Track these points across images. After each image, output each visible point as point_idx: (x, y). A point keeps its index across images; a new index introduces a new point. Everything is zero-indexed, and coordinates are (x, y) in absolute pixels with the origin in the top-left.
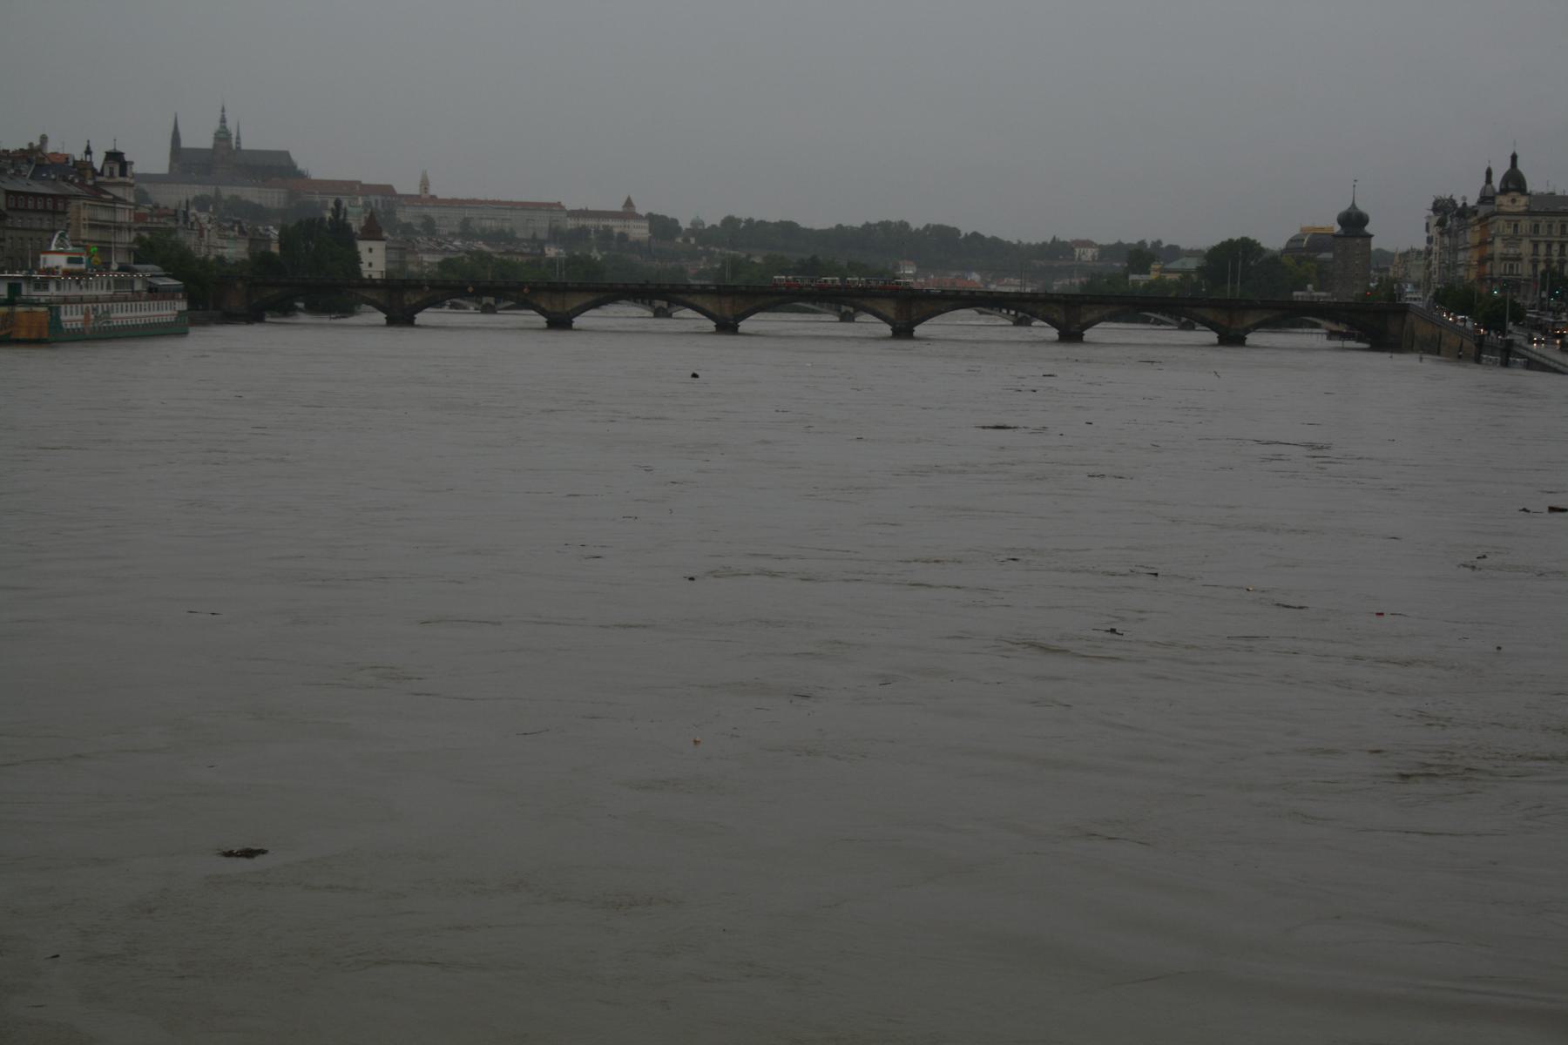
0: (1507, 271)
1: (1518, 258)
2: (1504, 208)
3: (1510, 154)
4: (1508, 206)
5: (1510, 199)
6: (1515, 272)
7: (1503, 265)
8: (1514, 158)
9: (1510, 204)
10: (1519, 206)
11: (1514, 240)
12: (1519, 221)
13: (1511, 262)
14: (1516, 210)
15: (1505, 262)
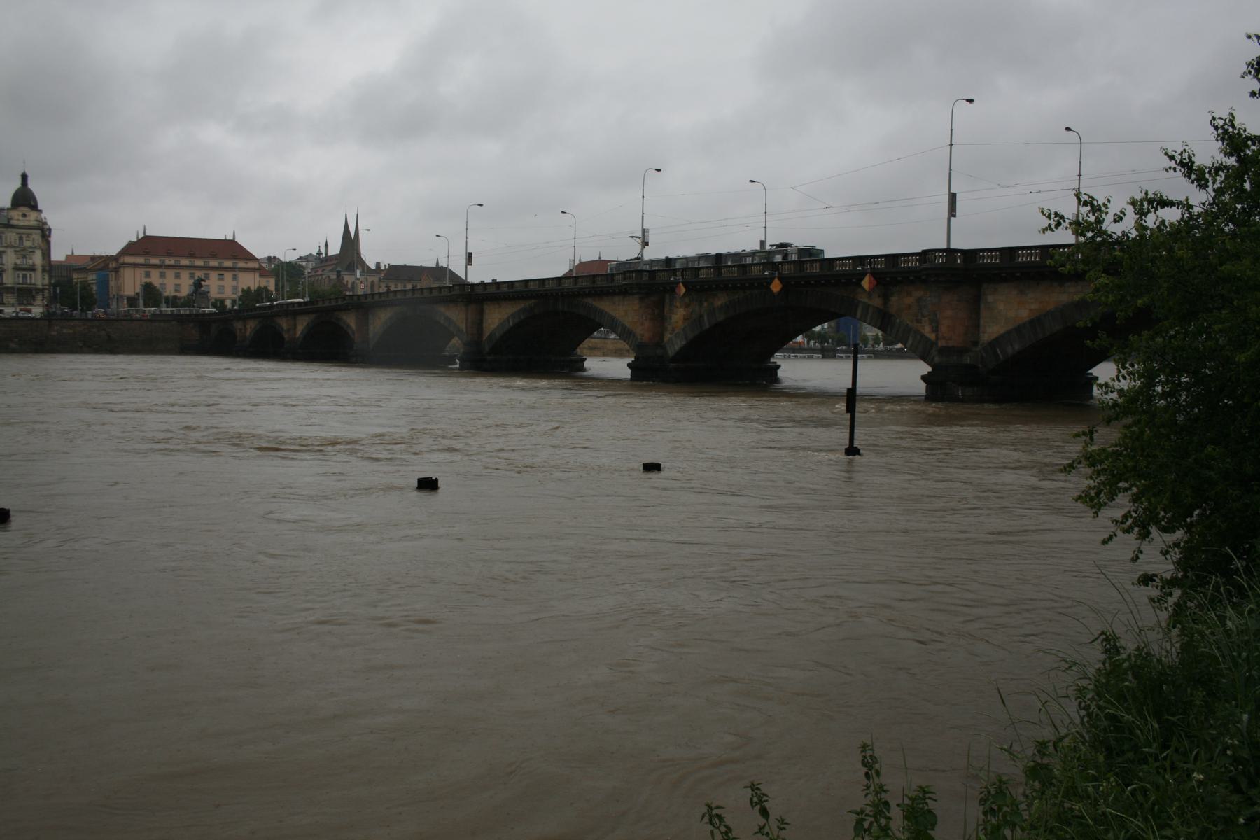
0: (21, 281)
1: (32, 269)
2: (14, 222)
3: (23, 171)
4: (18, 220)
5: (21, 213)
6: (28, 282)
7: (17, 275)
8: (24, 177)
9: (21, 218)
10: (29, 221)
11: (23, 252)
12: (31, 234)
13: (24, 272)
14: (26, 224)
15: (18, 272)
